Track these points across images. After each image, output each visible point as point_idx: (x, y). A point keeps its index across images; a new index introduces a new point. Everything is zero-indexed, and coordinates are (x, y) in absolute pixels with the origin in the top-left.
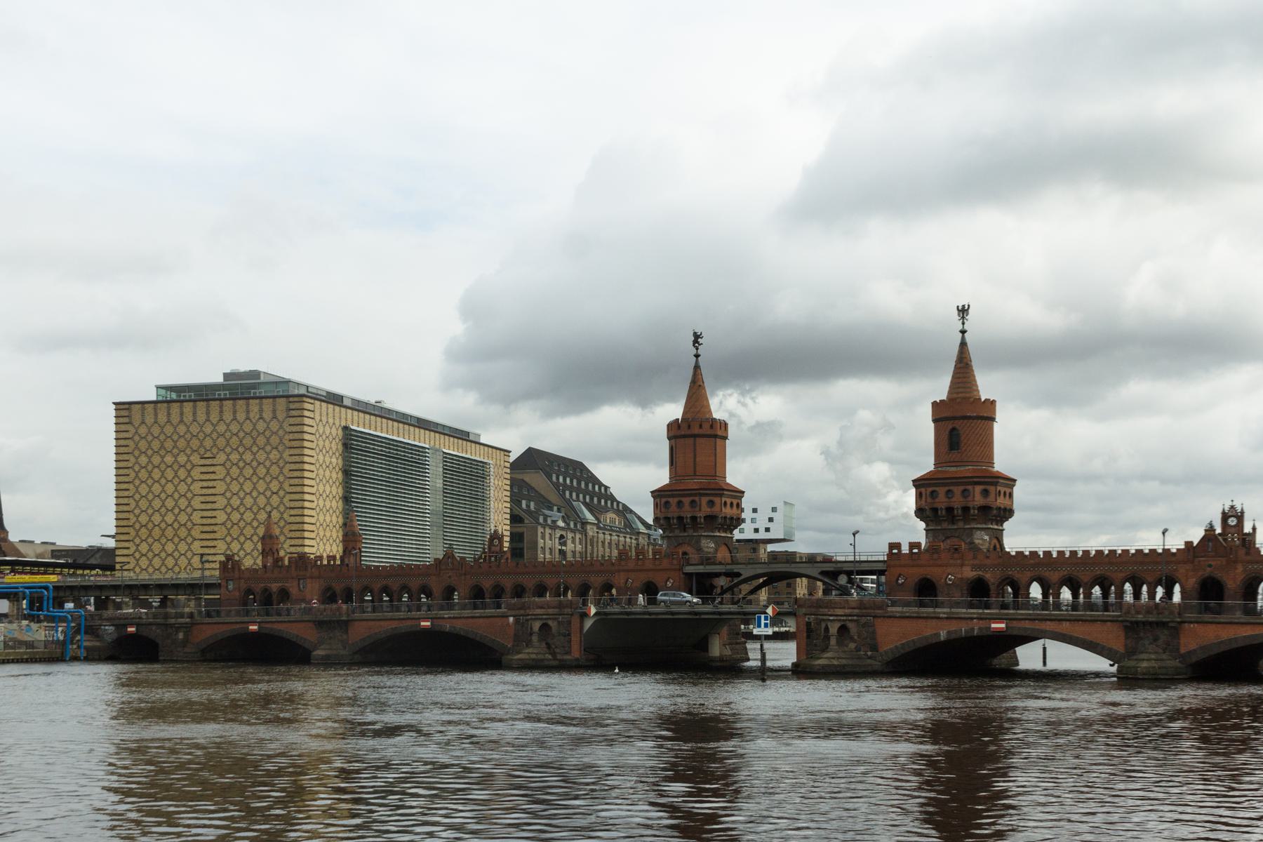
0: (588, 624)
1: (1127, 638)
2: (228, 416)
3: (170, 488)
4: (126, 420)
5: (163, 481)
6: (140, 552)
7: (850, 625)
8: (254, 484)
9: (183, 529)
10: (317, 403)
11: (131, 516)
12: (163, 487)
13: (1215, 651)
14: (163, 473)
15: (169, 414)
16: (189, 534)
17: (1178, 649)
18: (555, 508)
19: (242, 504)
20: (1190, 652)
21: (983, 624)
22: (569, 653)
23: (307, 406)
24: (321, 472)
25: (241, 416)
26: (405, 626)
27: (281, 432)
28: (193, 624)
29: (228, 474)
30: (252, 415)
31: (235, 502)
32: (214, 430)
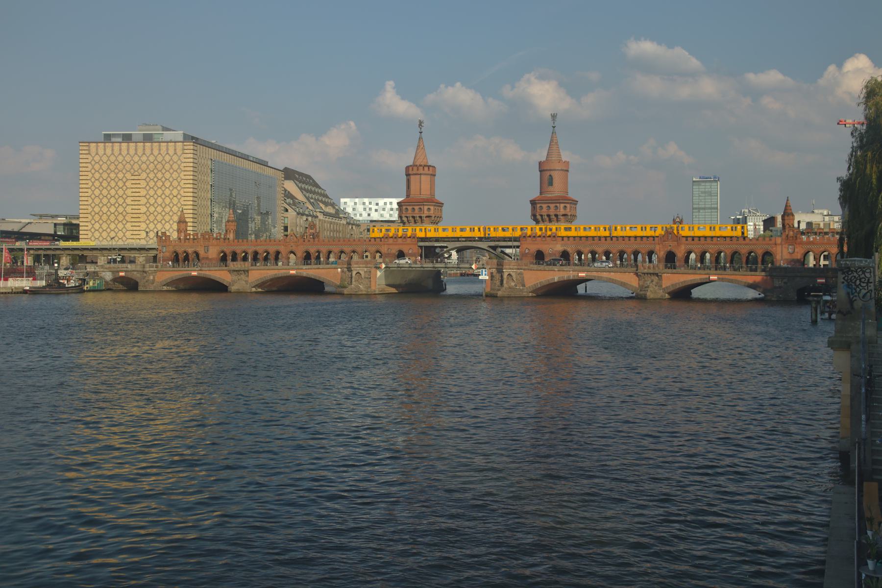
1: (639, 280)
3: (113, 192)
4: (86, 152)
6: (94, 229)
7: (513, 274)
8: (163, 191)
9: (121, 215)
10: (198, 146)
11: (89, 207)
12: (109, 191)
13: (678, 287)
14: (109, 183)
15: (113, 150)
16: (124, 219)
17: (661, 286)
19: (156, 202)
20: (667, 287)
21: (575, 273)
24: (200, 184)
25: (156, 152)
27: (179, 162)
29: (148, 184)
30: (162, 152)
31: (152, 201)
32: (140, 159)
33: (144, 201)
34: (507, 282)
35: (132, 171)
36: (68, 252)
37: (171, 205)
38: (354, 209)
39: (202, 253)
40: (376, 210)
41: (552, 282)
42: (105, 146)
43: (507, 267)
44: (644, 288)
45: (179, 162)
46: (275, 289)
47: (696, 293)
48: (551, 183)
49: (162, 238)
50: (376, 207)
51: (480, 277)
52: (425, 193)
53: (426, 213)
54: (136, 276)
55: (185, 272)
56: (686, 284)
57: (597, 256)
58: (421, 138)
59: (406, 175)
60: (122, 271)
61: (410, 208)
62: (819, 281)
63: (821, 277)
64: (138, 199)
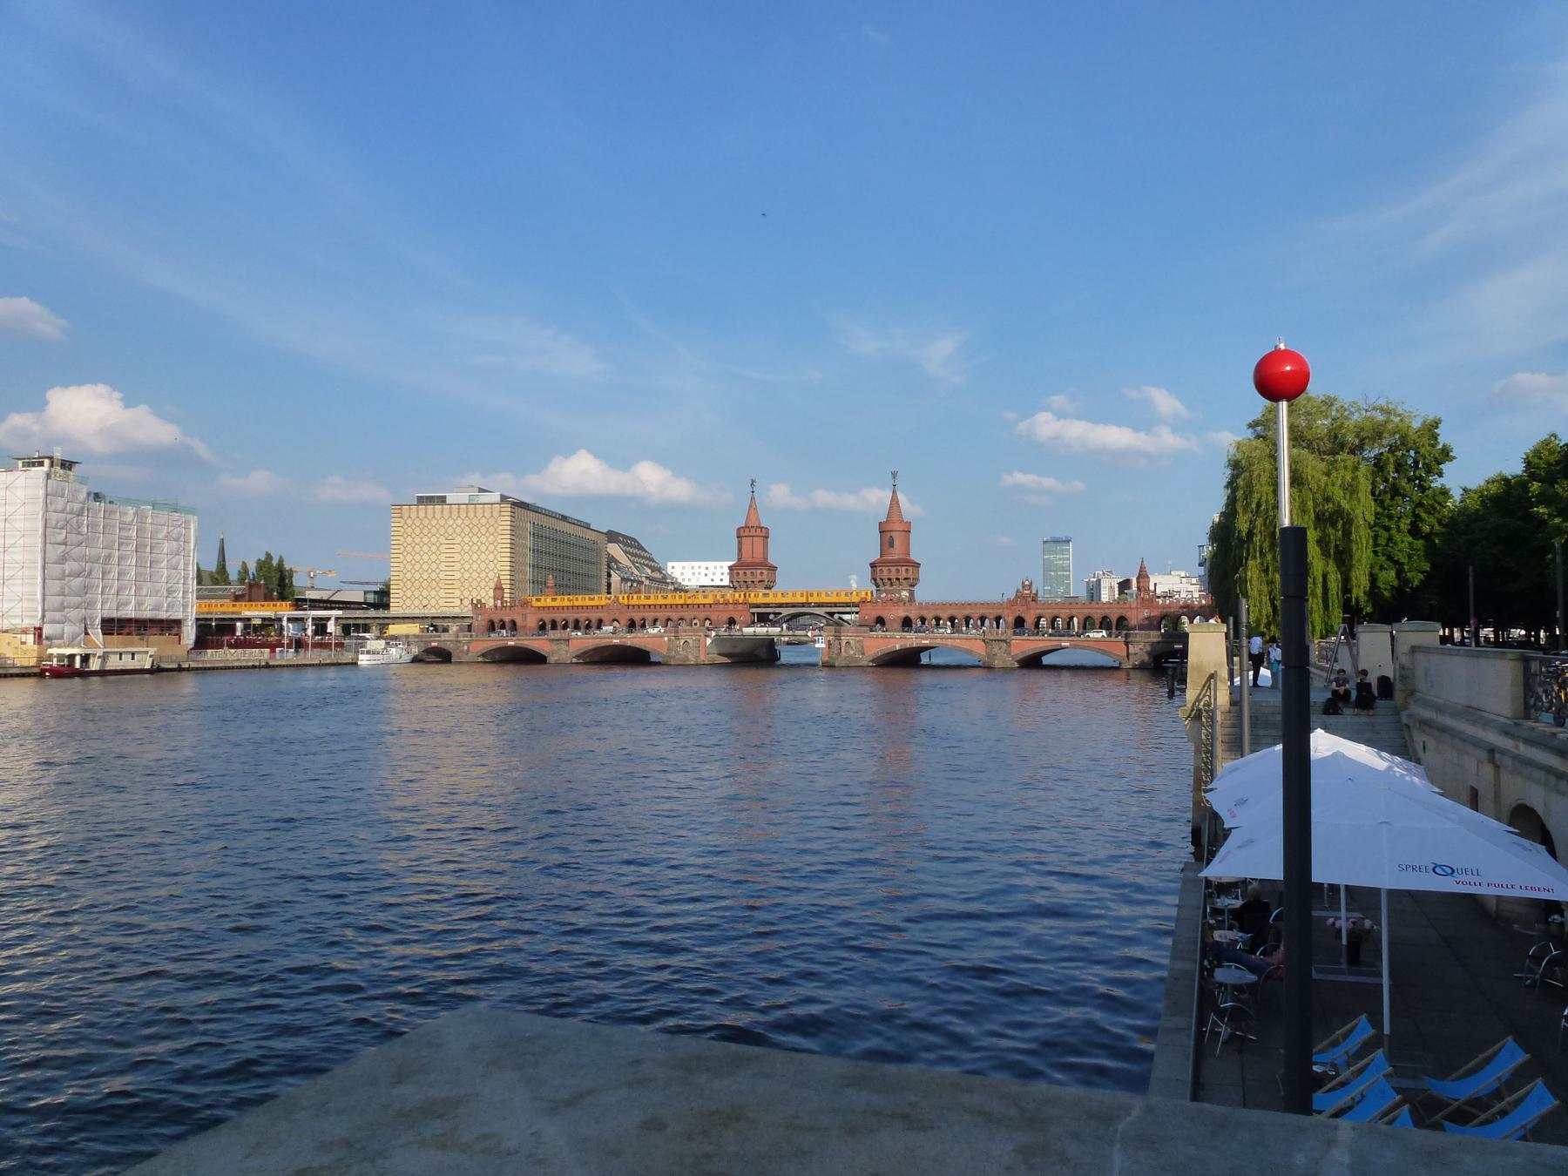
0: (709, 641)
2: (463, 515)
3: (426, 557)
4: (399, 515)
5: (422, 553)
17: (1010, 653)
25: (471, 515)
30: (477, 514)
33: (458, 566)
34: (846, 651)
36: (378, 621)
37: (487, 571)
38: (682, 574)
39: (519, 622)
40: (706, 575)
42: (418, 509)
43: (846, 634)
44: (991, 656)
45: (496, 525)
46: (596, 659)
47: (1046, 660)
48: (891, 545)
49: (478, 606)
50: (706, 572)
51: (817, 646)
52: (758, 557)
53: (759, 578)
54: (449, 646)
55: (498, 643)
57: (941, 622)
58: (753, 498)
59: (738, 537)
60: (434, 641)
61: (741, 572)
62: (1176, 646)
63: (1178, 643)
64: (452, 564)
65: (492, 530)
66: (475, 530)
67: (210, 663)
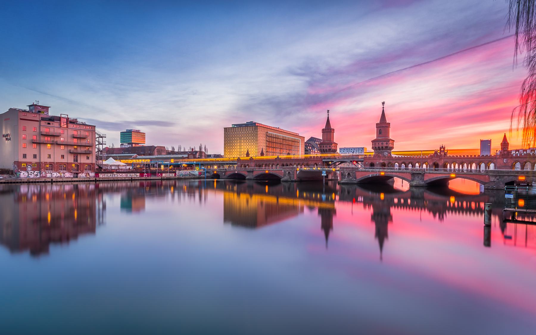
0: (298, 172)
1: (412, 177)
7: (350, 173)
13: (432, 180)
17: (424, 180)
18: (316, 149)
22: (294, 178)
23: (258, 128)
25: (246, 130)
26: (263, 172)
28: (226, 171)
35: (239, 137)
40: (351, 151)
41: (368, 177)
45: (254, 133)
51: (322, 175)
56: (437, 179)
61: (322, 146)
65: (252, 135)
66: (248, 135)
67: (120, 178)
